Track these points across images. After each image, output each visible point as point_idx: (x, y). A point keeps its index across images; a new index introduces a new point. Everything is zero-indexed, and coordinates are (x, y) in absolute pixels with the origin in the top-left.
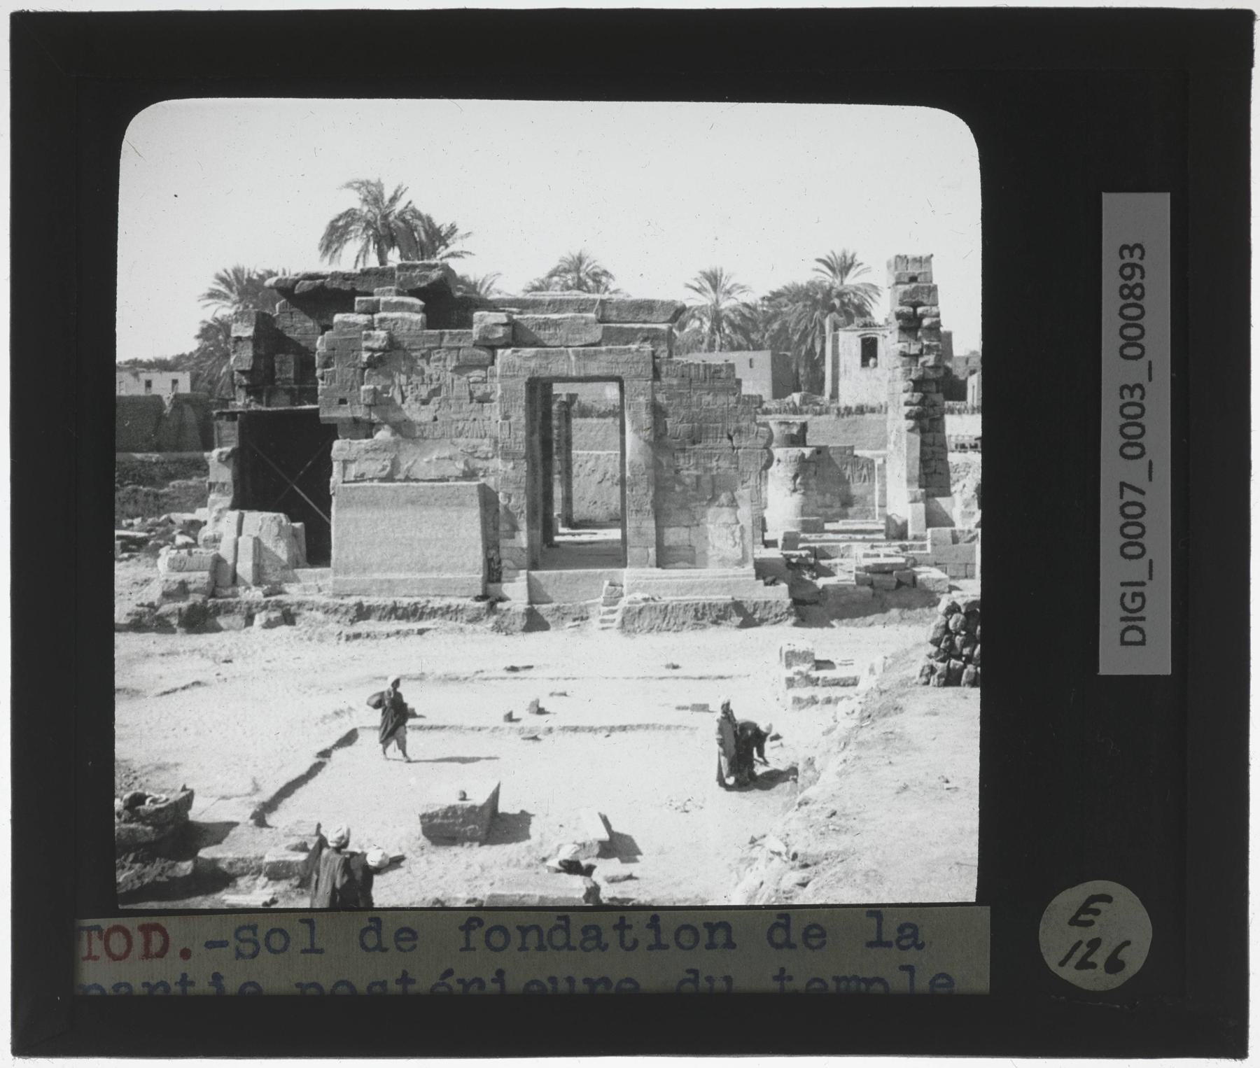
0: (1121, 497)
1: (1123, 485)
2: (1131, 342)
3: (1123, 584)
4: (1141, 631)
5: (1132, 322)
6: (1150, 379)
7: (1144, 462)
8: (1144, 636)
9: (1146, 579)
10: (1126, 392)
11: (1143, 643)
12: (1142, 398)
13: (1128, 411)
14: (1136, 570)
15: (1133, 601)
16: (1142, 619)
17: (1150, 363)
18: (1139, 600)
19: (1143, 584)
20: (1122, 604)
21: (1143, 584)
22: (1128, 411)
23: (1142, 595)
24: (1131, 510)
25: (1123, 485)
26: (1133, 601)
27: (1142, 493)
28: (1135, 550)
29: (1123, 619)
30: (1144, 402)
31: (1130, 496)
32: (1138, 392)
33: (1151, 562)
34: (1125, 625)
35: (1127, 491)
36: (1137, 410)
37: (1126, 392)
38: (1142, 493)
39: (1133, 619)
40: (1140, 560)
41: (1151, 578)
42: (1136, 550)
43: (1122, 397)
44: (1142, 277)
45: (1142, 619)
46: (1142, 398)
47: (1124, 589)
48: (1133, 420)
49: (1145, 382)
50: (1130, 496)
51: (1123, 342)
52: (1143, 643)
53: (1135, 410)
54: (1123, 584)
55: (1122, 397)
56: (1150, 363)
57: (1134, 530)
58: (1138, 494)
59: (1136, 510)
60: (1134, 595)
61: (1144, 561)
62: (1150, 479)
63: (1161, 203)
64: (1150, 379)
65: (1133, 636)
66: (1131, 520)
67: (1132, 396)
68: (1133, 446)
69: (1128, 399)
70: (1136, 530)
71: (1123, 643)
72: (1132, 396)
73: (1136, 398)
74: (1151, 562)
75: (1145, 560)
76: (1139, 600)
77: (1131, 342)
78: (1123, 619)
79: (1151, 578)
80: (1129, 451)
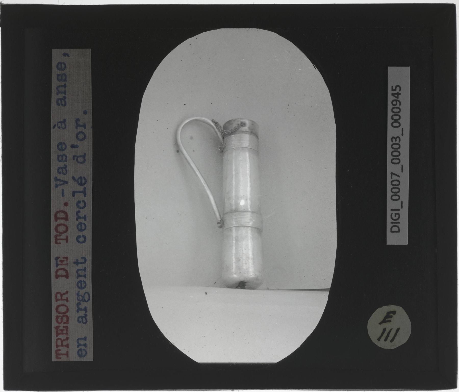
0: (392, 178)
1: (392, 174)
2: (396, 121)
3: (392, 210)
4: (398, 227)
5: (396, 114)
6: (402, 135)
7: (399, 166)
8: (399, 229)
9: (400, 208)
10: (394, 140)
11: (399, 231)
12: (399, 142)
13: (394, 146)
14: (396, 205)
15: (395, 216)
16: (399, 223)
17: (402, 129)
18: (397, 216)
19: (399, 210)
20: (392, 218)
21: (399, 210)
22: (394, 146)
23: (398, 214)
24: (394, 183)
25: (392, 174)
26: (395, 216)
27: (399, 176)
28: (397, 198)
29: (392, 223)
30: (400, 143)
31: (395, 177)
32: (398, 139)
33: (402, 202)
34: (392, 225)
35: (393, 175)
36: (397, 146)
37: (394, 140)
38: (399, 176)
39: (396, 222)
40: (398, 201)
41: (402, 207)
42: (397, 198)
43: (392, 141)
44: (400, 90)
45: (399, 223)
46: (399, 142)
47: (392, 212)
48: (396, 150)
49: (401, 136)
50: (395, 177)
51: (393, 121)
52: (399, 231)
53: (397, 146)
54: (392, 210)
55: (392, 141)
56: (402, 129)
57: (397, 190)
58: (398, 177)
59: (396, 183)
60: (396, 214)
61: (399, 202)
62: (402, 172)
63: (406, 71)
64: (402, 135)
65: (395, 229)
66: (395, 187)
67: (396, 141)
68: (397, 159)
69: (394, 142)
70: (397, 190)
71: (392, 232)
72: (396, 141)
73: (397, 142)
74: (402, 202)
75: (400, 201)
76: (397, 216)
77: (396, 121)
78: (392, 223)
79: (402, 207)
80: (395, 161)
